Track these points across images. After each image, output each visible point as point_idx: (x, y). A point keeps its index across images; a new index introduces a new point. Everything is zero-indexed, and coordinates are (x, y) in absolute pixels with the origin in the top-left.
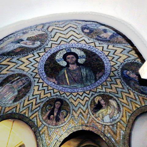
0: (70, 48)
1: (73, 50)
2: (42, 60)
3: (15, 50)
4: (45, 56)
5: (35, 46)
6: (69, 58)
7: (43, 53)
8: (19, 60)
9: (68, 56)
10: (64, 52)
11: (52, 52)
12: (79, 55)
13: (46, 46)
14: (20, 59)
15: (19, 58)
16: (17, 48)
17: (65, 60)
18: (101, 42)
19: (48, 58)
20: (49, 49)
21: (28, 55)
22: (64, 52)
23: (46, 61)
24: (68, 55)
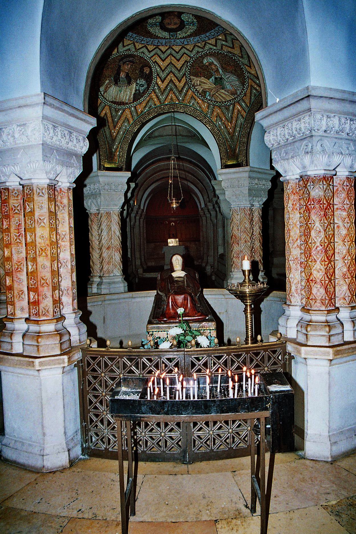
0: (170, 38)
1: (166, 34)
2: (217, 33)
3: (232, 73)
4: (209, 37)
5: (211, 59)
6: (175, 24)
7: (210, 42)
8: (242, 55)
9: (174, 27)
10: (180, 34)
11: (197, 38)
12: (159, 28)
13: (200, 50)
14: (240, 55)
15: (240, 57)
16: (228, 72)
17: (182, 22)
18: (127, 53)
19: (207, 32)
20: (199, 44)
21: (229, 52)
22: (180, 34)
23: (212, 30)
24: (176, 28)
